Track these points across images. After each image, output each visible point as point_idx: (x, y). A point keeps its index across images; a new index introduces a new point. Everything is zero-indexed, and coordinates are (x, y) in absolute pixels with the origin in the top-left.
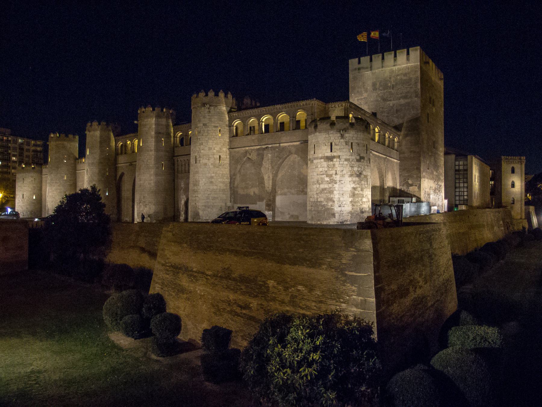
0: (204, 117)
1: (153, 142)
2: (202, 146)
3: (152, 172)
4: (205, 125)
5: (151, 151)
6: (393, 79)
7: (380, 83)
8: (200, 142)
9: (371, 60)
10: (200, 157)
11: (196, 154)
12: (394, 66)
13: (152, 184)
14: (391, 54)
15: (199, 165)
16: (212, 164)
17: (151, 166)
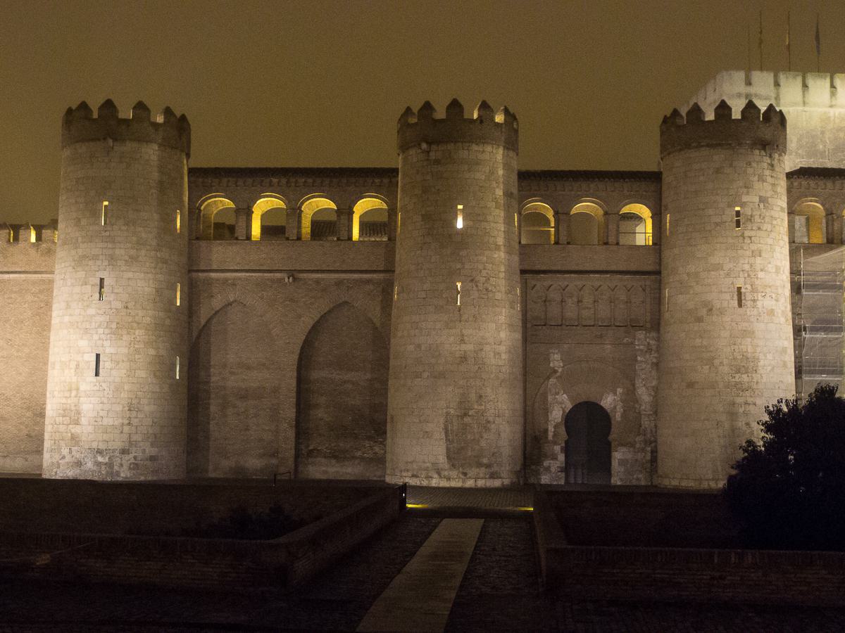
0: (762, 179)
1: (501, 220)
2: (758, 260)
3: (502, 319)
4: (763, 200)
5: (497, 248)
6: (828, 135)
7: (799, 140)
8: (754, 247)
9: (777, 84)
10: (754, 290)
11: (740, 283)
12: (831, 106)
13: (504, 356)
14: (826, 76)
15: (755, 312)
16: (783, 311)
17: (499, 296)
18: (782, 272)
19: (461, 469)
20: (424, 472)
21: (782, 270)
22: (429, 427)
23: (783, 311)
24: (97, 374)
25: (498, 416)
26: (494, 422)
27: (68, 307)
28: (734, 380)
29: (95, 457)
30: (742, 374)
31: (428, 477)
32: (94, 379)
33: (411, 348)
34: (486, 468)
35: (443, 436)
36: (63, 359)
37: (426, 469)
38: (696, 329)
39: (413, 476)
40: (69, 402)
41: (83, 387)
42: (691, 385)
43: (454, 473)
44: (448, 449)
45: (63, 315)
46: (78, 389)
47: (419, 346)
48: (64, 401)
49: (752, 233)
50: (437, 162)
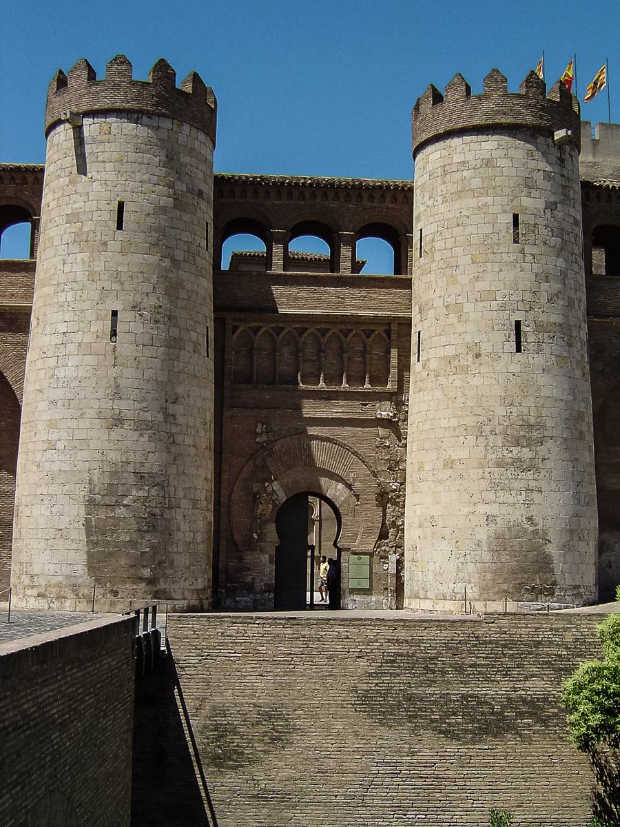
2: (545, 286)
18: (577, 307)
19: (108, 585)
20: (54, 590)
21: (576, 304)
22: (64, 522)
23: (577, 361)
25: (170, 508)
26: (162, 516)
28: (510, 455)
30: (523, 447)
34: (147, 584)
35: (84, 537)
37: (59, 585)
38: (458, 383)
39: (40, 595)
42: (449, 464)
44: (90, 555)
47: (54, 402)
49: (535, 250)
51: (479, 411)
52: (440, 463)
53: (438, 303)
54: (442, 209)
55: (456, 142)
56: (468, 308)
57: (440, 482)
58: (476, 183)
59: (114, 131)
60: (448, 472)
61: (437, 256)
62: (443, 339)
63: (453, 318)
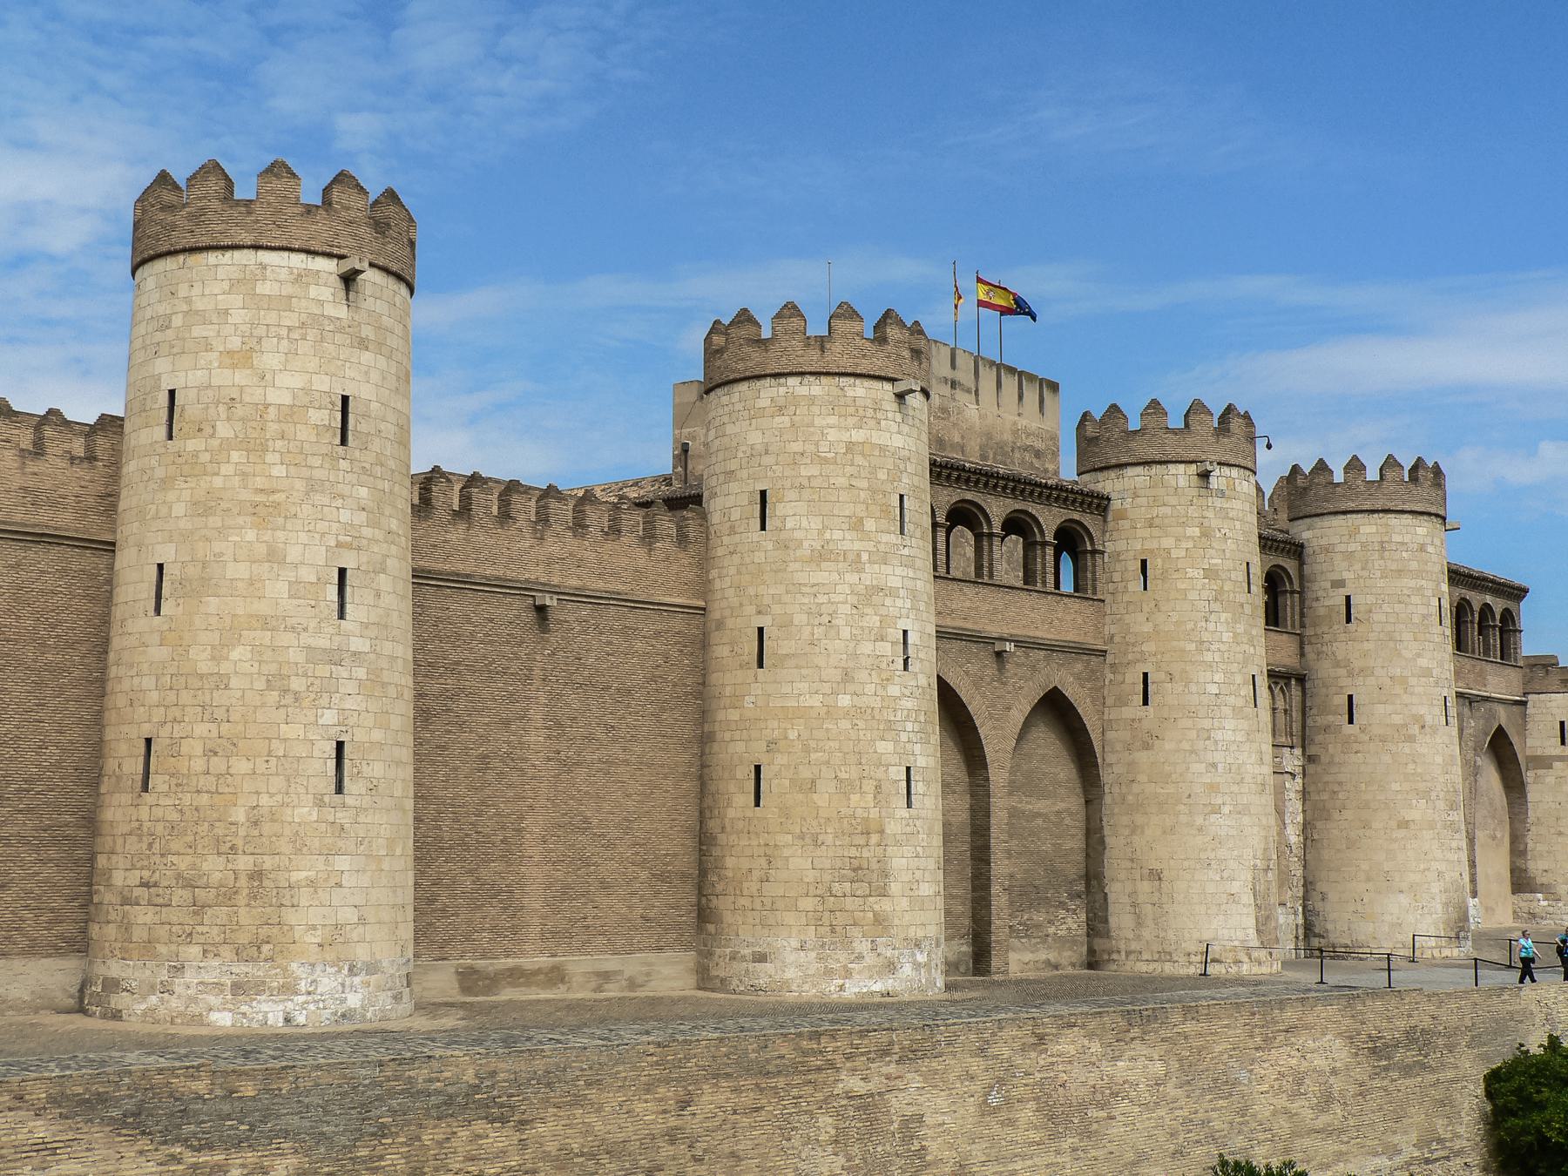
6: (1017, 455)
22: (1235, 887)
24: (909, 805)
27: (847, 677)
29: (913, 955)
31: (1238, 962)
32: (905, 813)
33: (1201, 767)
36: (843, 775)
38: (1407, 750)
40: (866, 854)
41: (892, 828)
42: (1403, 824)
43: (1263, 954)
45: (835, 693)
46: (882, 832)
47: (1214, 765)
48: (853, 852)
50: (1221, 494)
51: (1428, 777)
52: (1393, 824)
53: (1379, 672)
54: (1381, 583)
55: (1392, 520)
56: (1413, 681)
57: (1396, 840)
58: (1414, 565)
59: (1238, 488)
60: (1402, 833)
61: (1377, 627)
62: (1389, 708)
63: (1398, 690)
